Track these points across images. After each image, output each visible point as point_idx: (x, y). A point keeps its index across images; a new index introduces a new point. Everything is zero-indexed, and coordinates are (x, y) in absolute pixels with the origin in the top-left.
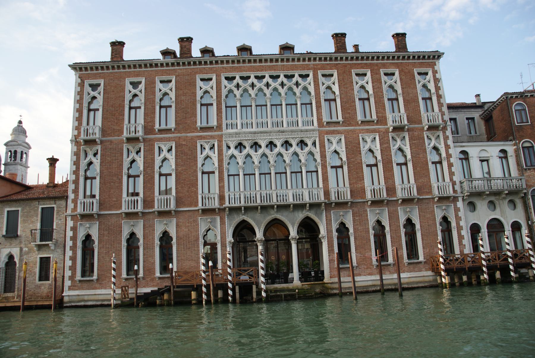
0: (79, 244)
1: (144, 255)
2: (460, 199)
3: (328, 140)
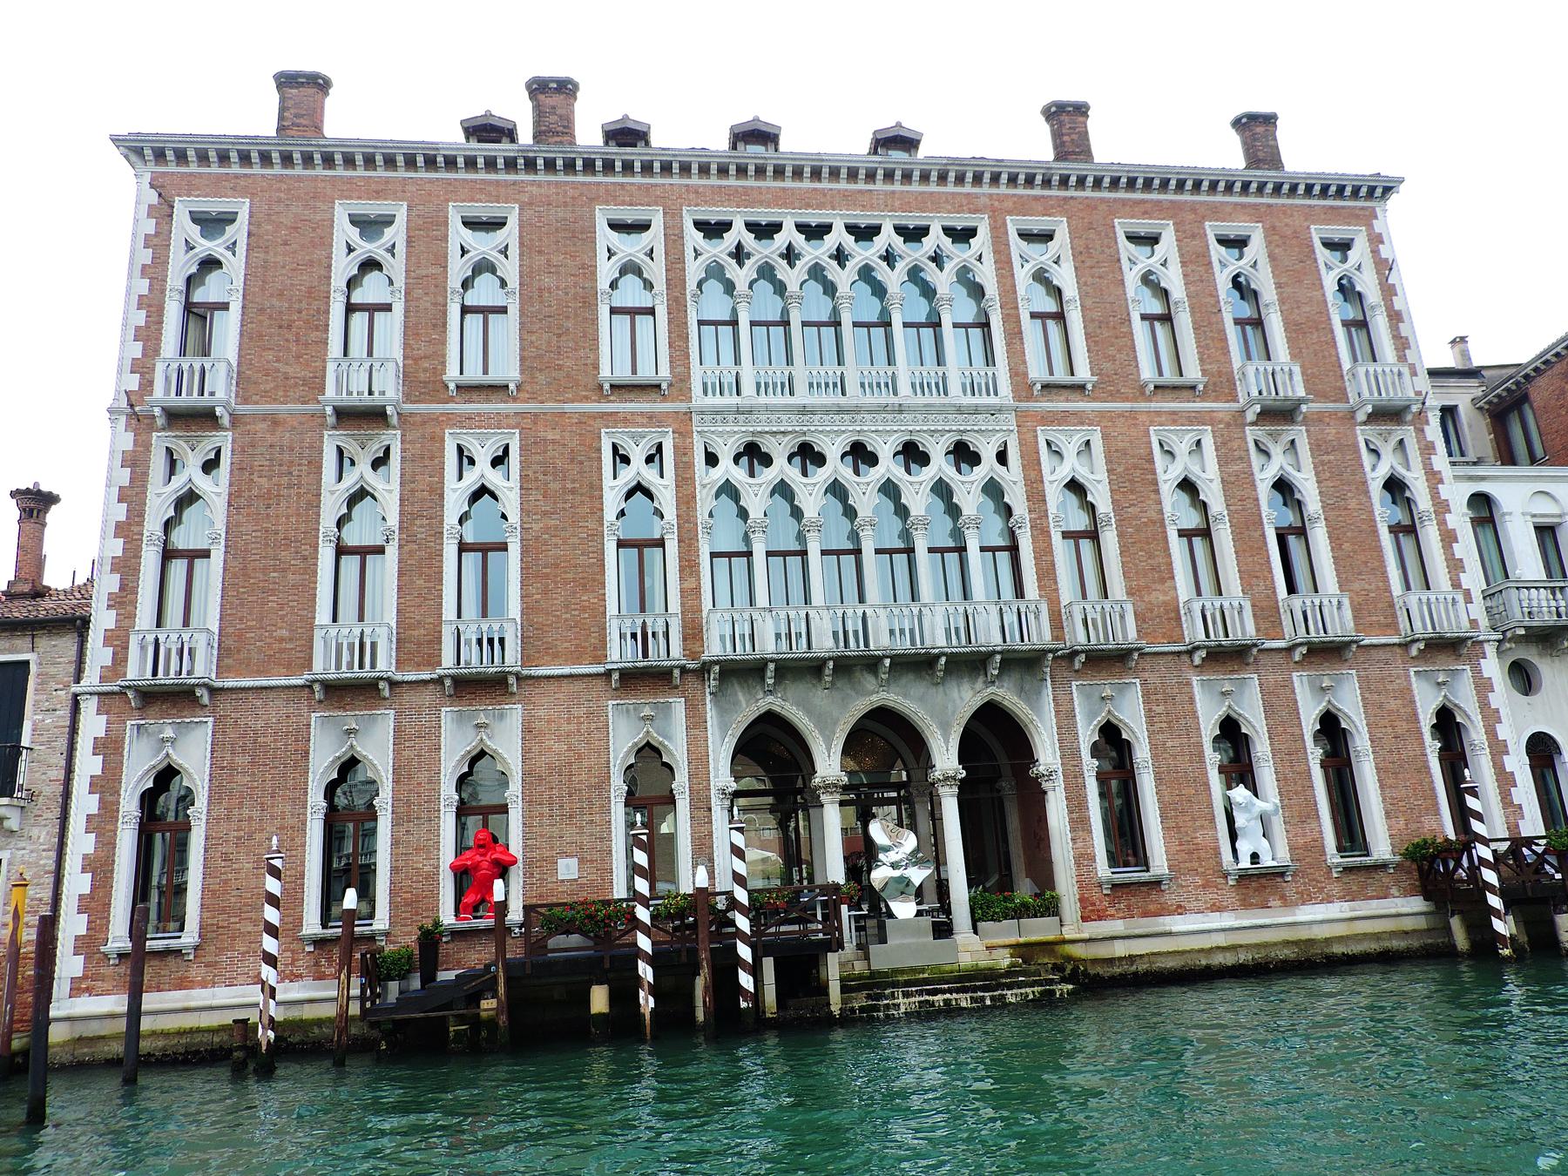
0: (129, 806)
1: (395, 843)
2: (1490, 650)
3: (1049, 444)
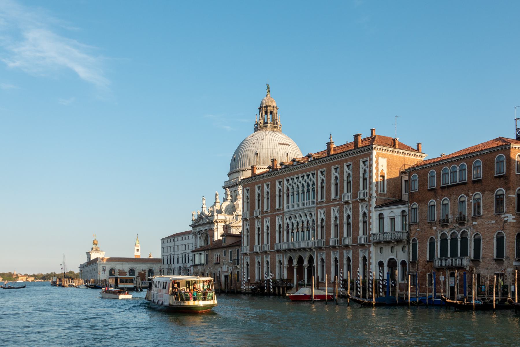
0: (245, 266)
2: (372, 246)
